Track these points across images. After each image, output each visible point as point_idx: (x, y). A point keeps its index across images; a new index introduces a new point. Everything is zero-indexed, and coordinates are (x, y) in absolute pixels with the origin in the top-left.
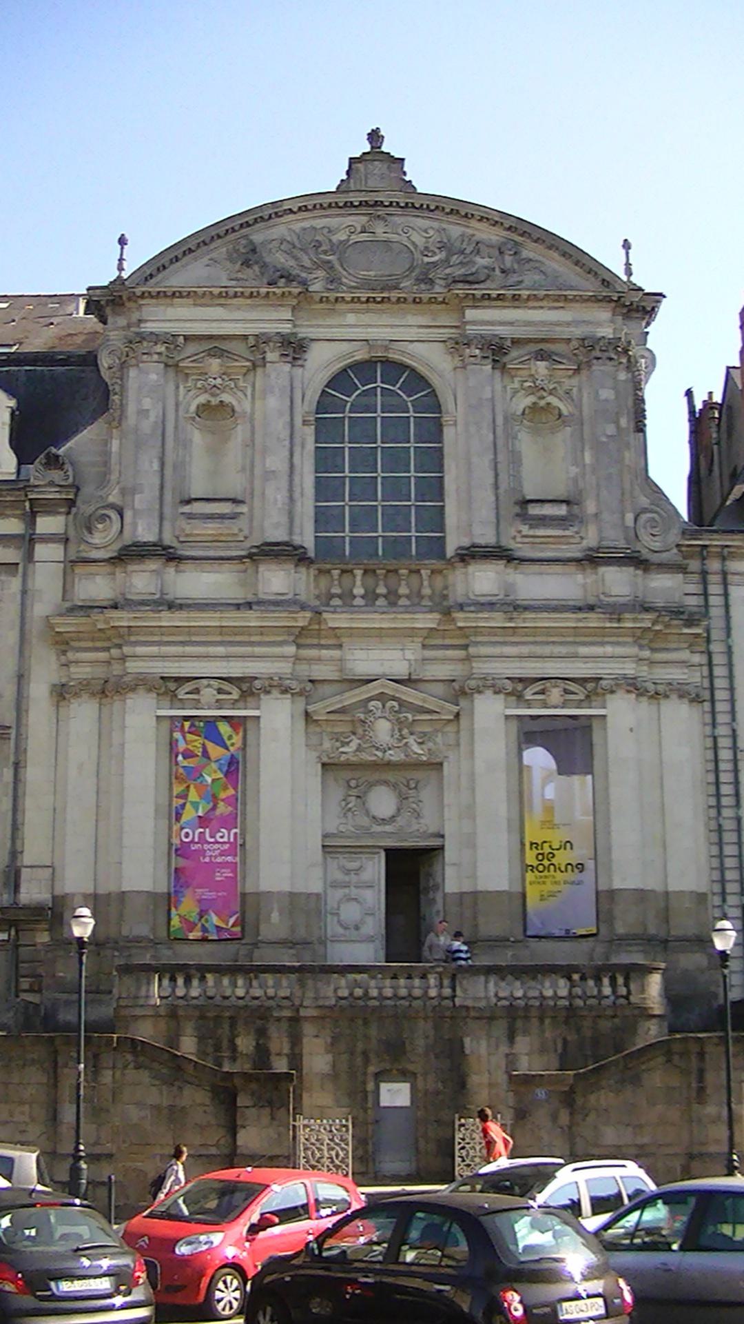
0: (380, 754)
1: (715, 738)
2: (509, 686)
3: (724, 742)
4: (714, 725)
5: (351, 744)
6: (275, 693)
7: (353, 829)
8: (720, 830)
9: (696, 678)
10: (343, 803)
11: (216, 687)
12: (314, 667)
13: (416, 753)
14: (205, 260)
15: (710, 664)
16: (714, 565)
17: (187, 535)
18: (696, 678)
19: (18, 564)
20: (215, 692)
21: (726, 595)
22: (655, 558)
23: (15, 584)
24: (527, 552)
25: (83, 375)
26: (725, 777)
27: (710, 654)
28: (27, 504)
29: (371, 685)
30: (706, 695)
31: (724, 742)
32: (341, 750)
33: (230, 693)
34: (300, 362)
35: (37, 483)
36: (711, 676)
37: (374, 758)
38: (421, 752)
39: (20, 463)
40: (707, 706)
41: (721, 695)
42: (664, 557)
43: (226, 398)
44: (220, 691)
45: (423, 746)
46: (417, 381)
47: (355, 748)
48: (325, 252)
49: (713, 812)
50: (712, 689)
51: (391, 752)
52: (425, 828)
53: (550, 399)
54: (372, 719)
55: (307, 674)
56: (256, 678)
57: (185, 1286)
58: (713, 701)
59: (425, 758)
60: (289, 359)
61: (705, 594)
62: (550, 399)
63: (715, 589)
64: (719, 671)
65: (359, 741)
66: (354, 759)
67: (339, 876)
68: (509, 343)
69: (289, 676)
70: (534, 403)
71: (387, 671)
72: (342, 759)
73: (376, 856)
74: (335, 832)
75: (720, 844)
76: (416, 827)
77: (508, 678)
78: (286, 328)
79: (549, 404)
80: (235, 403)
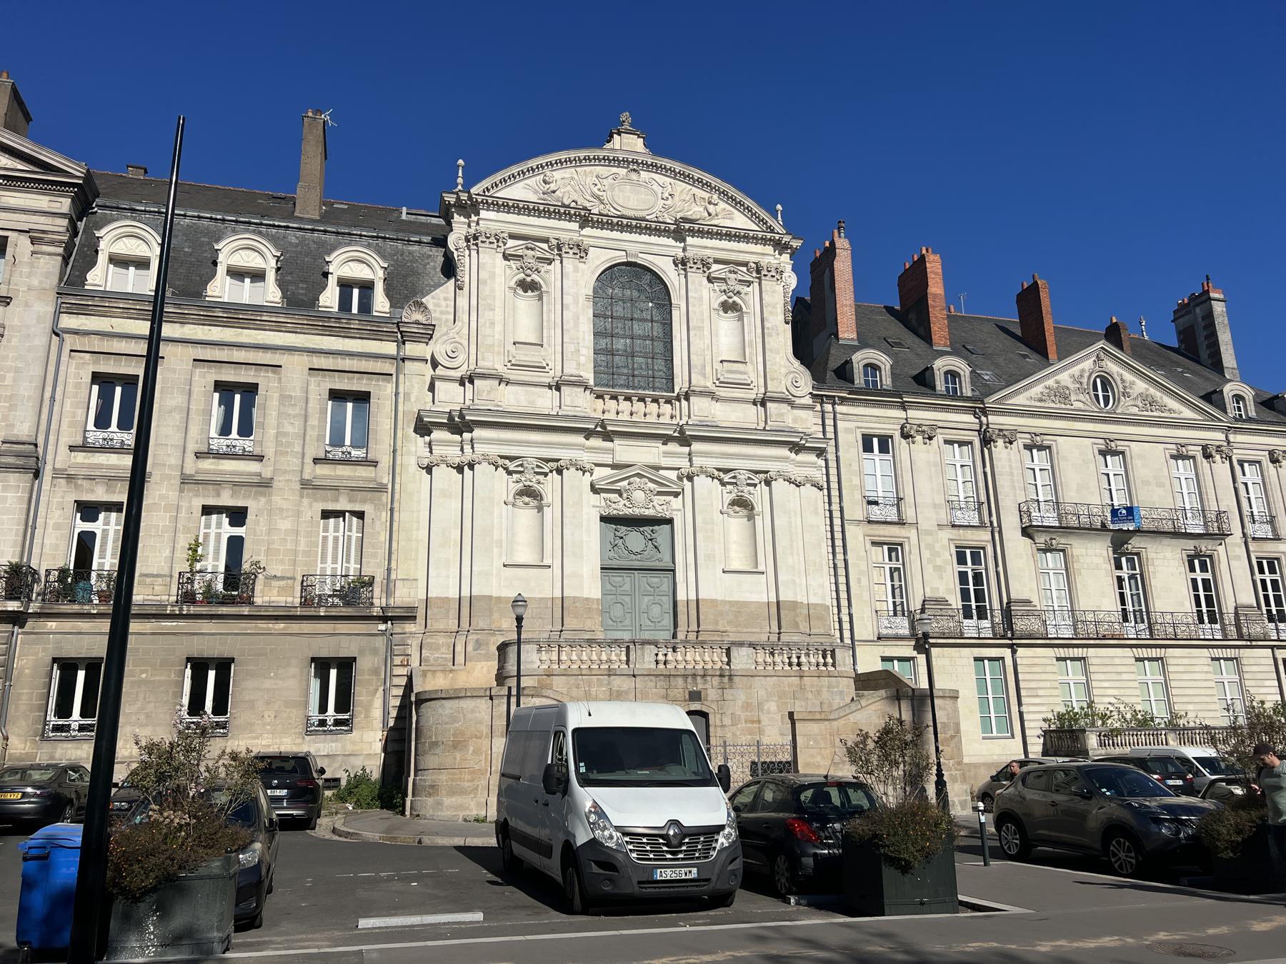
1: (831, 512)
2: (716, 473)
3: (837, 514)
4: (830, 503)
6: (573, 469)
8: (835, 567)
9: (820, 476)
14: (522, 184)
15: (827, 467)
16: (828, 407)
17: (513, 365)
18: (820, 476)
19: (391, 375)
21: (835, 426)
22: (798, 401)
23: (389, 388)
24: (722, 392)
25: (431, 253)
26: (838, 535)
27: (826, 461)
28: (399, 336)
30: (825, 486)
31: (837, 514)
34: (583, 260)
35: (406, 320)
36: (828, 475)
39: (391, 306)
40: (826, 492)
41: (834, 485)
42: (803, 401)
43: (535, 277)
46: (657, 279)
48: (599, 190)
49: (831, 556)
50: (828, 481)
53: (736, 299)
57: (488, 882)
58: (829, 489)
60: (578, 257)
61: (824, 425)
62: (736, 299)
63: (829, 422)
64: (833, 471)
67: (609, 586)
68: (711, 260)
70: (726, 301)
75: (836, 575)
78: (575, 237)
79: (734, 302)
80: (542, 282)
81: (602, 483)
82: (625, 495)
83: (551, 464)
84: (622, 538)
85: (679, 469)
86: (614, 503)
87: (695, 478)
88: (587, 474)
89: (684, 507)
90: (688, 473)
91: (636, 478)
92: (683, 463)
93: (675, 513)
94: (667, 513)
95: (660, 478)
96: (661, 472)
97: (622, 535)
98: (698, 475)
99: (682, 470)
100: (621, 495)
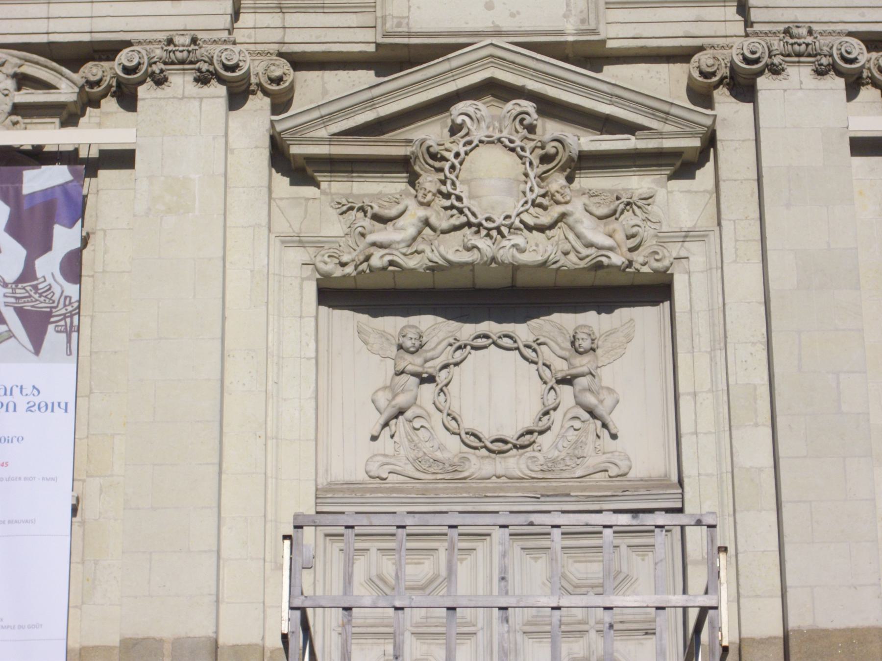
0: (483, 243)
5: (401, 222)
7: (410, 470)
10: (383, 399)
11: (9, 69)
12: (293, 19)
13: (589, 245)
20: (10, 84)
29: (456, 60)
32: (371, 238)
33: (53, 87)
37: (466, 257)
38: (608, 242)
44: (23, 81)
45: (613, 225)
47: (411, 231)
51: (518, 240)
52: (624, 465)
54: (462, 150)
55: (277, 36)
56: (128, 44)
59: (617, 259)
65: (422, 212)
66: (412, 263)
69: (224, 35)
71: (507, 24)
72: (377, 261)
73: (479, 545)
74: (361, 476)
76: (593, 461)
77: (850, 34)
81: (323, 133)
82: (429, 181)
83: (92, 70)
84: (431, 379)
85: (682, 56)
86: (377, 218)
87: (763, 83)
88: (258, 104)
89: (719, 224)
90: (733, 67)
91: (483, 108)
92: (721, 29)
93: (675, 250)
94: (638, 258)
95: (613, 98)
96: (612, 73)
97: (431, 367)
98: (776, 70)
99: (704, 59)
100: (413, 180)
